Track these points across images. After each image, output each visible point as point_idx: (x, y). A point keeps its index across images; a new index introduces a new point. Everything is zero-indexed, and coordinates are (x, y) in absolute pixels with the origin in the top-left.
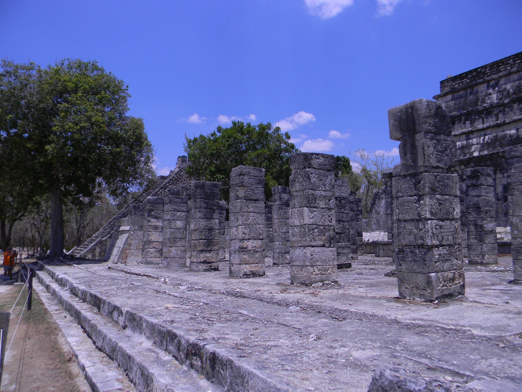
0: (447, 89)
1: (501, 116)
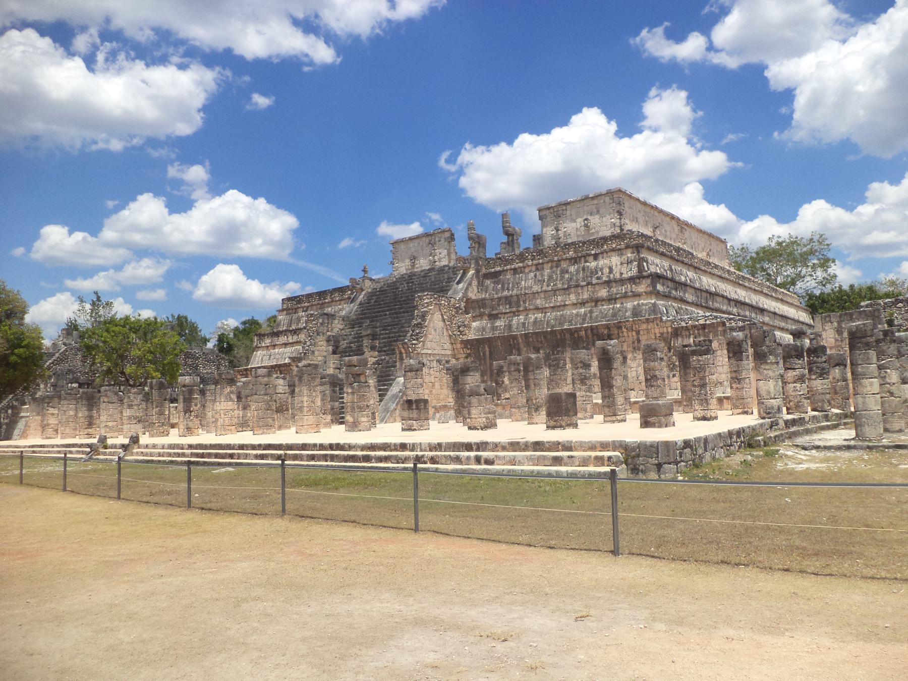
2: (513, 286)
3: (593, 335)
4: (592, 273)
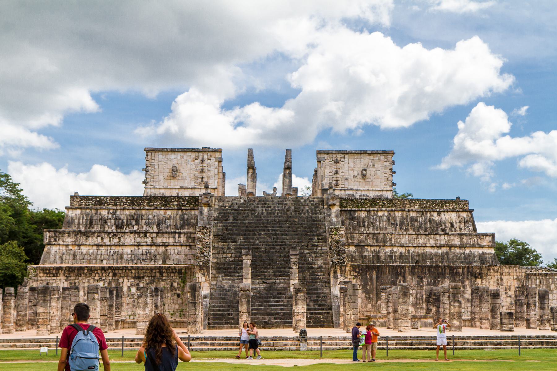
0: (76, 204)
1: (122, 239)
2: (369, 225)
3: (468, 272)
4: (437, 225)
